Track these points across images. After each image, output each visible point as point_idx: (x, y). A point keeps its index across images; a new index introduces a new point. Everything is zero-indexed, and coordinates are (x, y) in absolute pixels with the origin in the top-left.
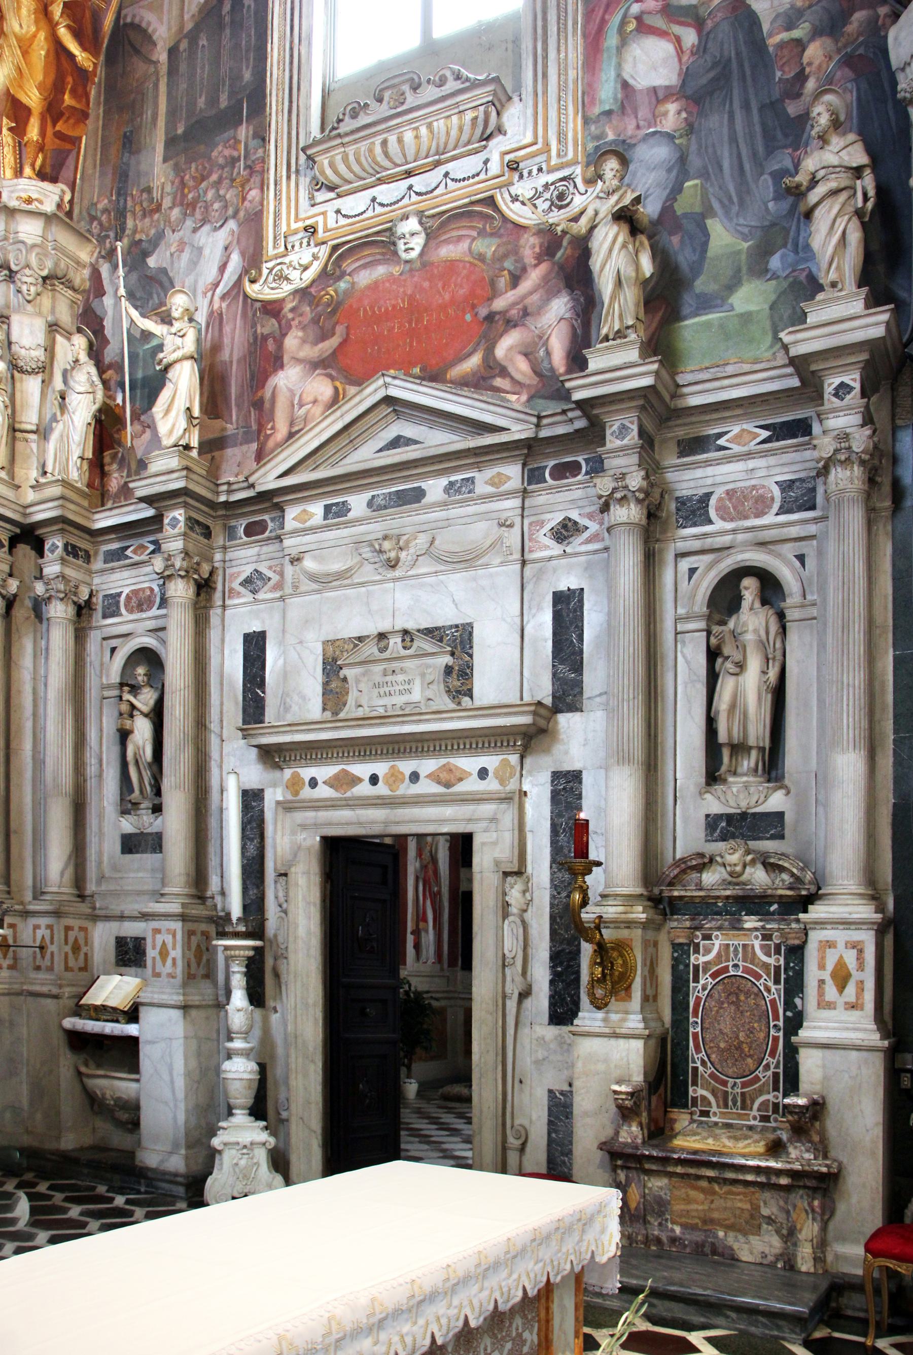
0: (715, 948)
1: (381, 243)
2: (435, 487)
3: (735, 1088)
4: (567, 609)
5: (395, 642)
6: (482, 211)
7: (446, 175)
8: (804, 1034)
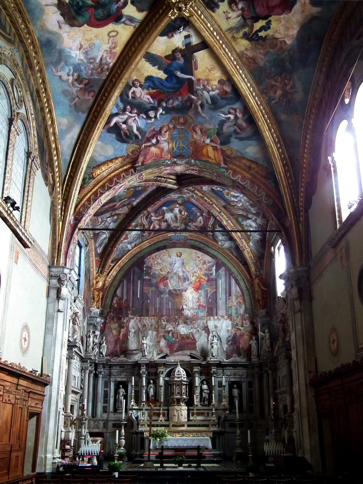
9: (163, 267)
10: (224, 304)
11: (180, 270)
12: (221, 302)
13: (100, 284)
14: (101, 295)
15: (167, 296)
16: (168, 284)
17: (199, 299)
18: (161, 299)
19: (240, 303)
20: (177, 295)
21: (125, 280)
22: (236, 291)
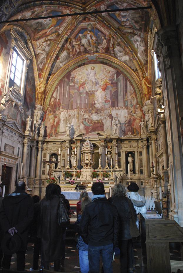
9: (83, 77)
10: (123, 99)
11: (93, 78)
12: (120, 98)
13: (42, 90)
14: (43, 97)
15: (85, 95)
16: (85, 88)
17: (106, 96)
18: (81, 97)
19: (133, 97)
20: (91, 94)
21: (59, 87)
22: (130, 89)
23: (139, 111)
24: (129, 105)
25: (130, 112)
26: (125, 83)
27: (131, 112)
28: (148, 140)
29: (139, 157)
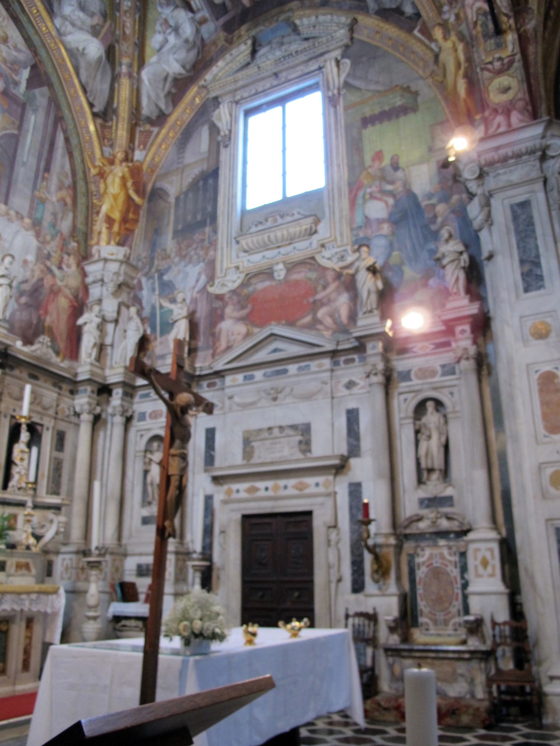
0: (426, 555)
1: (268, 273)
2: (293, 368)
3: (440, 616)
4: (352, 417)
5: (276, 432)
6: (310, 262)
7: (294, 248)
8: (470, 589)
10: (31, 185)
19: (66, 204)
22: (63, 167)
23: (74, 267)
24: (46, 223)
25: (45, 252)
26: (50, 128)
27: (49, 257)
28: (104, 390)
29: (56, 454)
